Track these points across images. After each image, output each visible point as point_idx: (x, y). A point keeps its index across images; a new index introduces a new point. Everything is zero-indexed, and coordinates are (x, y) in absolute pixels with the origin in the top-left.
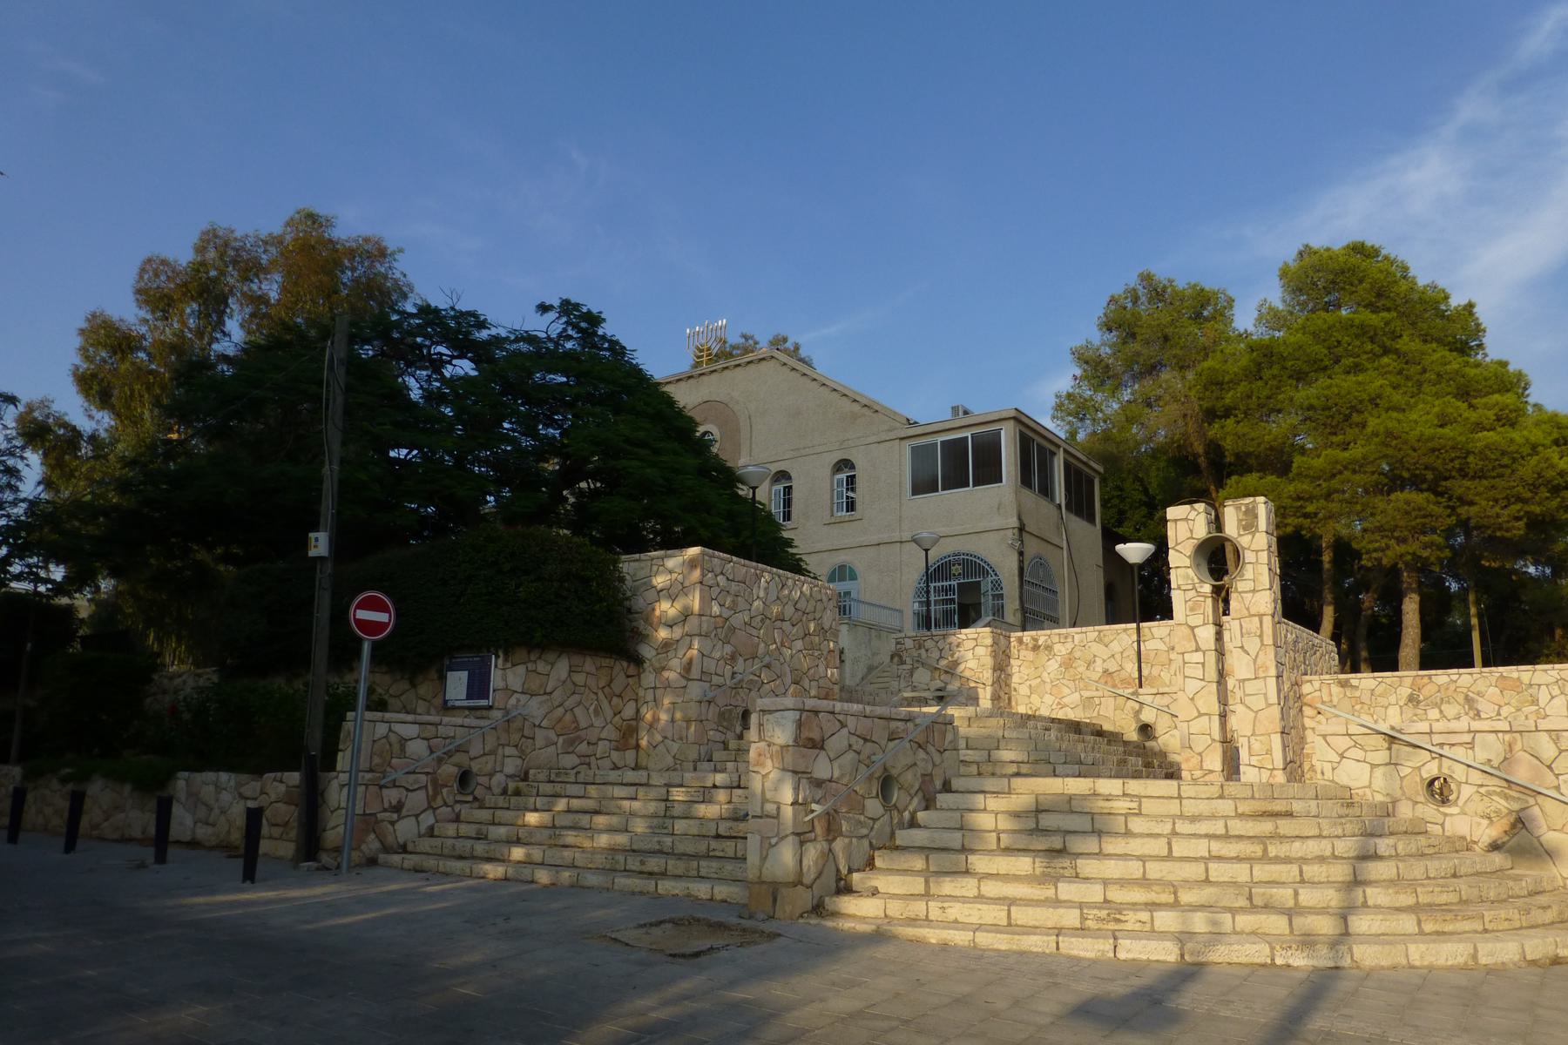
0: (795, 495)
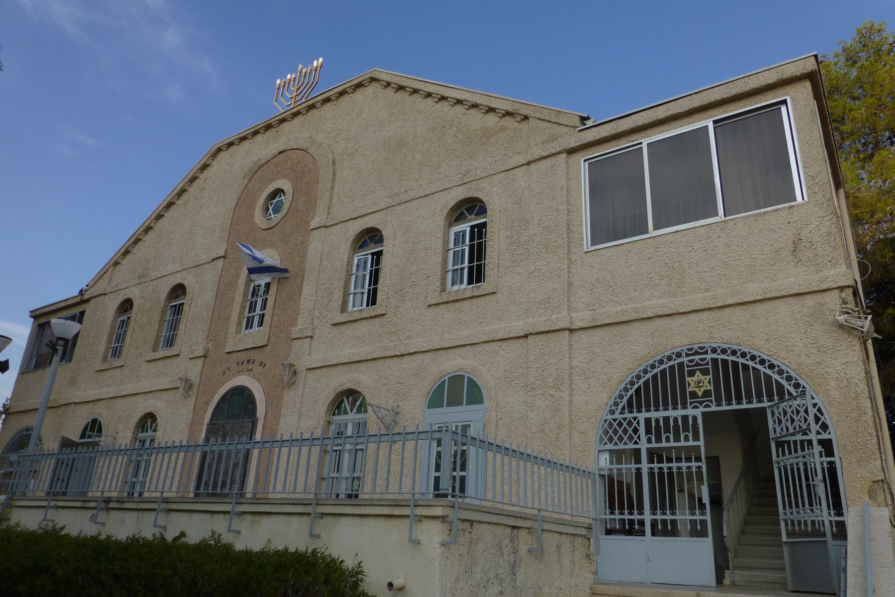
0: (385, 260)
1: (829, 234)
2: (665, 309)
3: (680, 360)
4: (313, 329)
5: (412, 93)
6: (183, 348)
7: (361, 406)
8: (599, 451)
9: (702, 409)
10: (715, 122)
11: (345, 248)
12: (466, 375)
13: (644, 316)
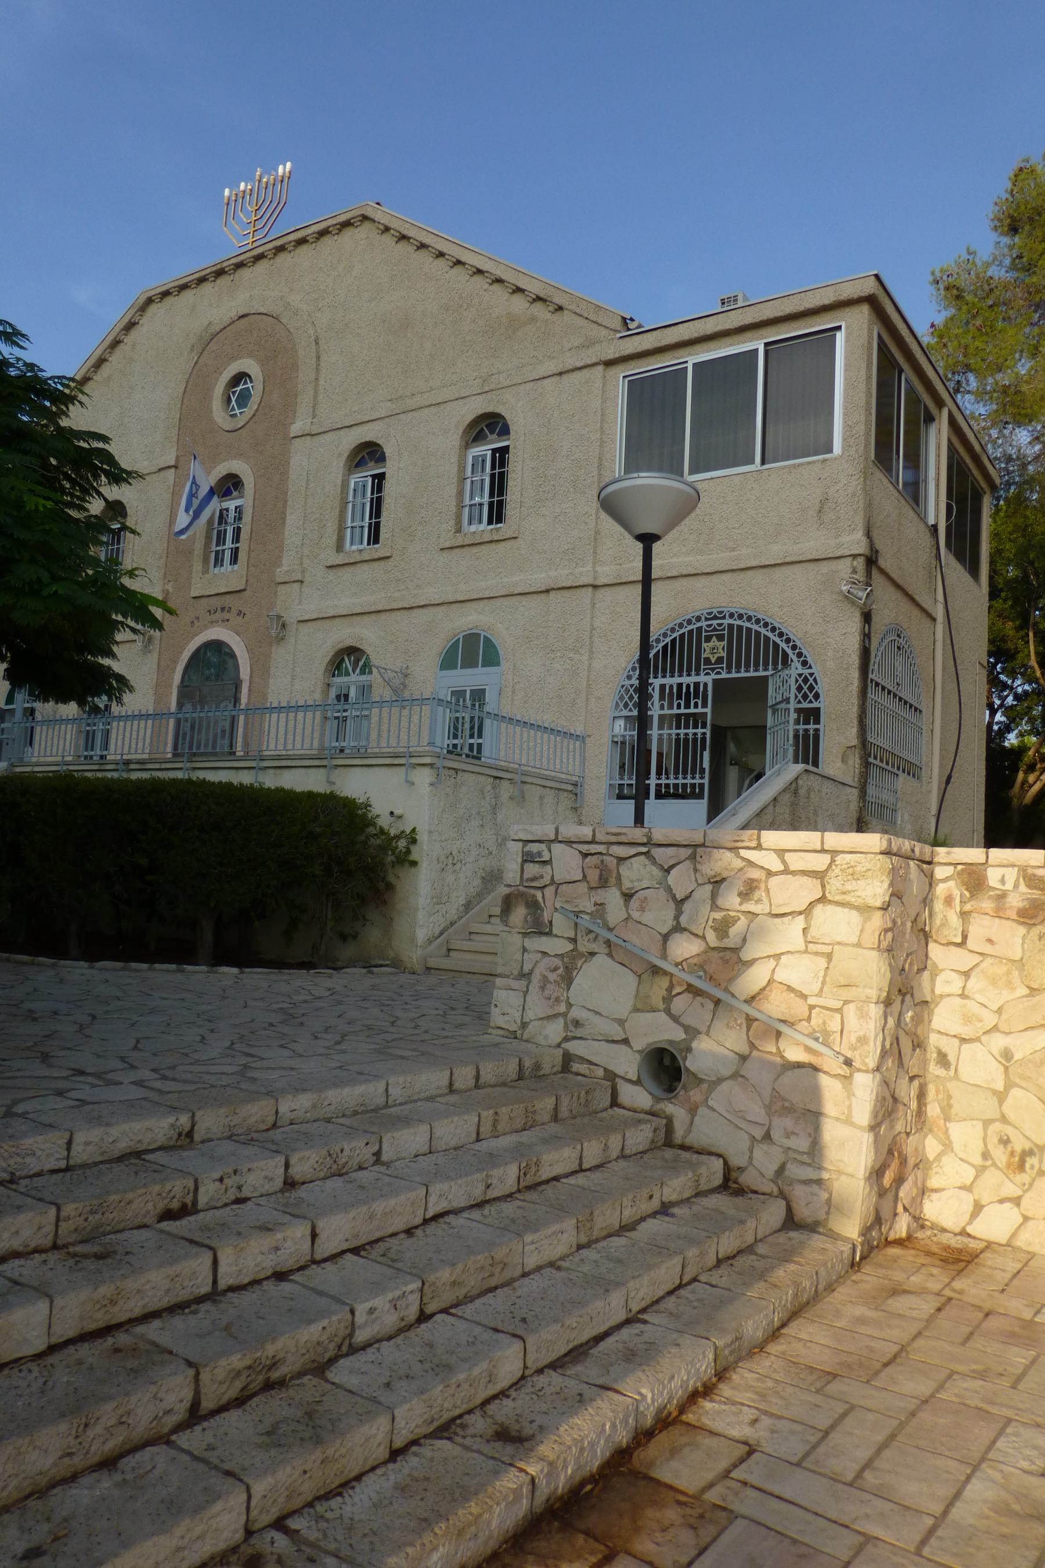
0: (388, 485)
1: (854, 495)
2: (690, 569)
3: (699, 625)
4: (303, 572)
5: (418, 248)
7: (364, 666)
8: (614, 718)
9: (714, 676)
10: (766, 344)
11: (338, 466)
12: (483, 634)
13: (669, 575)
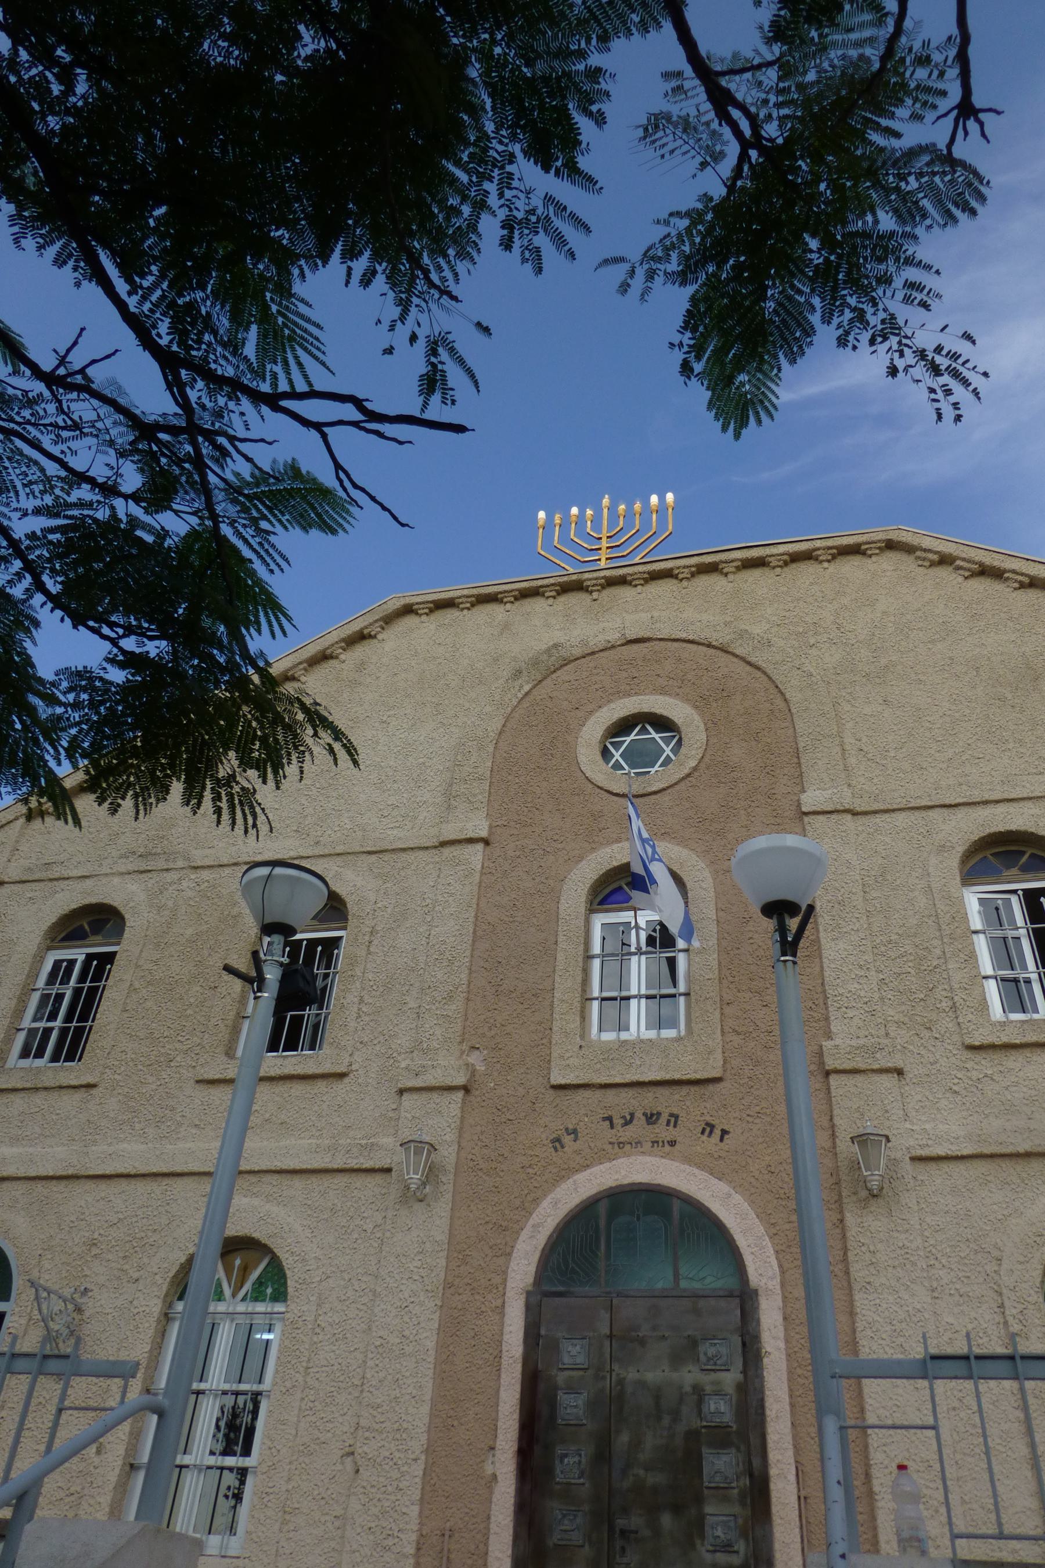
6: (358, 1057)
